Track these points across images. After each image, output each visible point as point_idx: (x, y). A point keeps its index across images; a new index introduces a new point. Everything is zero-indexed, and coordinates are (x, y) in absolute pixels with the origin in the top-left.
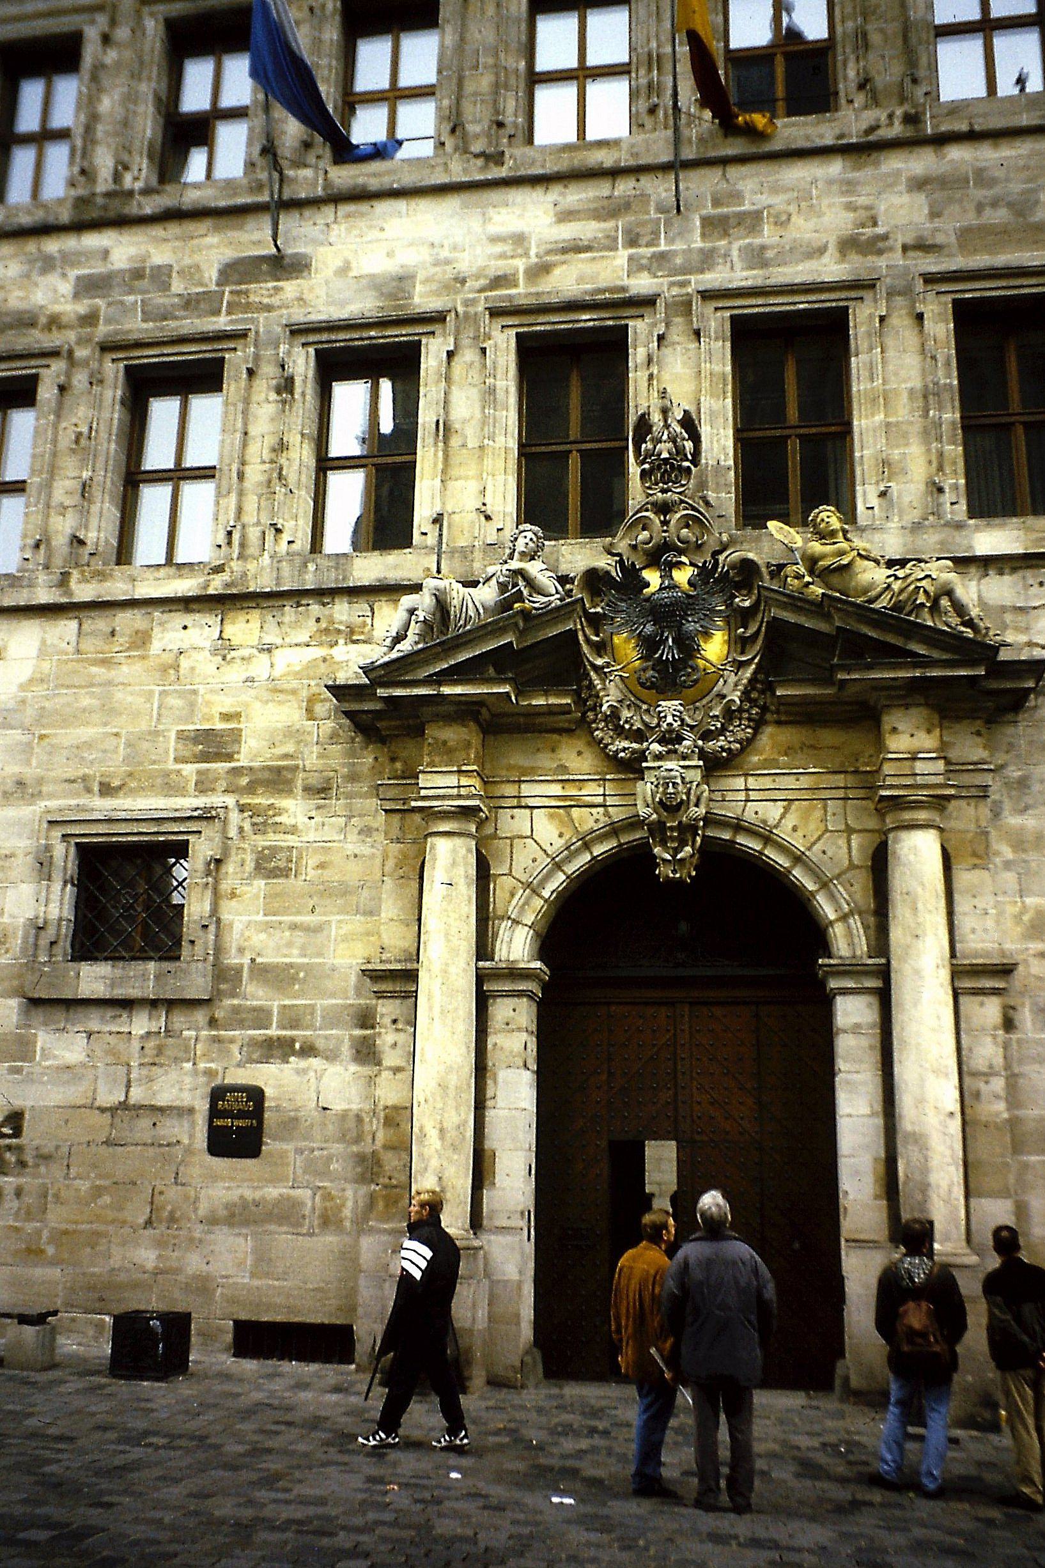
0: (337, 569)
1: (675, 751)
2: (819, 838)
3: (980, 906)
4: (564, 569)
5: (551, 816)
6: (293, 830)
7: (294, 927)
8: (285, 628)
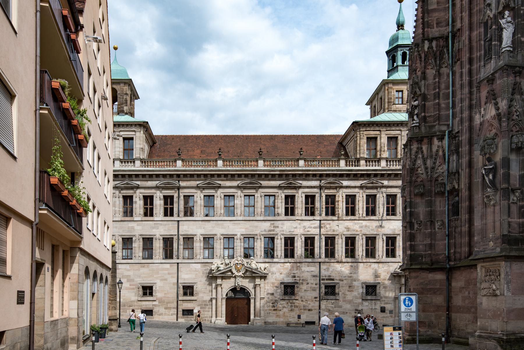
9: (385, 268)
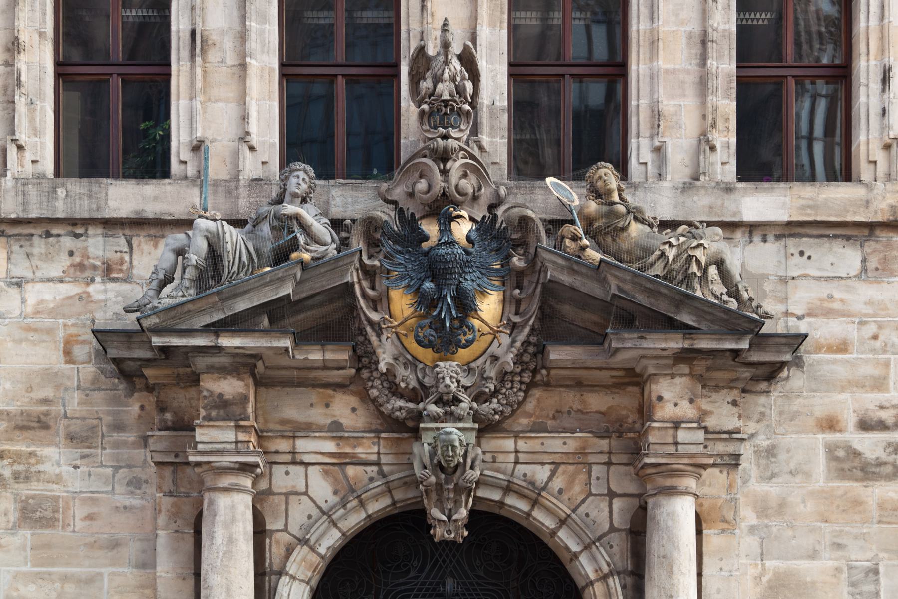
0: (90, 197)
1: (452, 414)
2: (583, 501)
3: (725, 568)
4: (336, 211)
5: (326, 472)
6: (58, 479)
7: (65, 578)
8: (36, 261)
9: (36, 293)
